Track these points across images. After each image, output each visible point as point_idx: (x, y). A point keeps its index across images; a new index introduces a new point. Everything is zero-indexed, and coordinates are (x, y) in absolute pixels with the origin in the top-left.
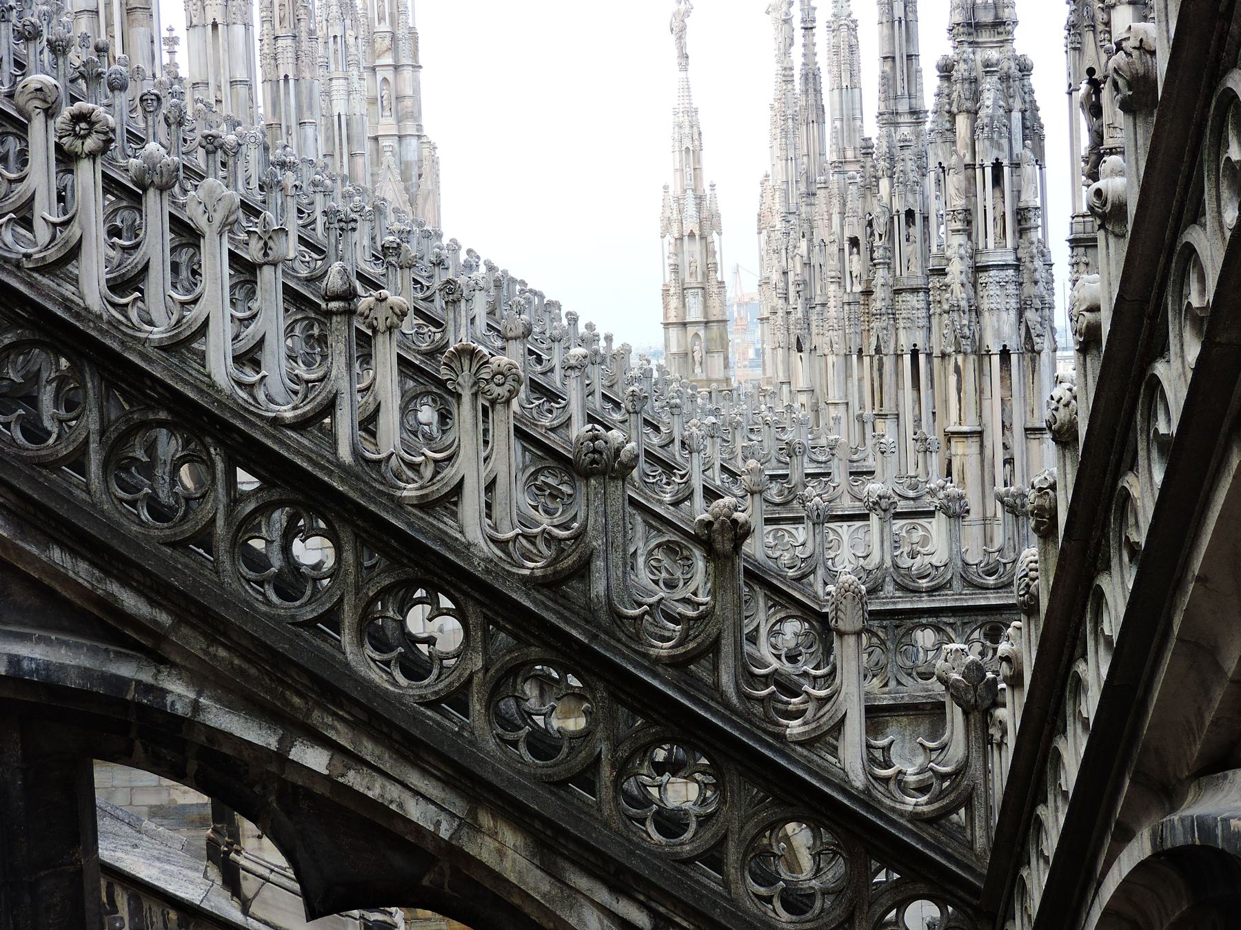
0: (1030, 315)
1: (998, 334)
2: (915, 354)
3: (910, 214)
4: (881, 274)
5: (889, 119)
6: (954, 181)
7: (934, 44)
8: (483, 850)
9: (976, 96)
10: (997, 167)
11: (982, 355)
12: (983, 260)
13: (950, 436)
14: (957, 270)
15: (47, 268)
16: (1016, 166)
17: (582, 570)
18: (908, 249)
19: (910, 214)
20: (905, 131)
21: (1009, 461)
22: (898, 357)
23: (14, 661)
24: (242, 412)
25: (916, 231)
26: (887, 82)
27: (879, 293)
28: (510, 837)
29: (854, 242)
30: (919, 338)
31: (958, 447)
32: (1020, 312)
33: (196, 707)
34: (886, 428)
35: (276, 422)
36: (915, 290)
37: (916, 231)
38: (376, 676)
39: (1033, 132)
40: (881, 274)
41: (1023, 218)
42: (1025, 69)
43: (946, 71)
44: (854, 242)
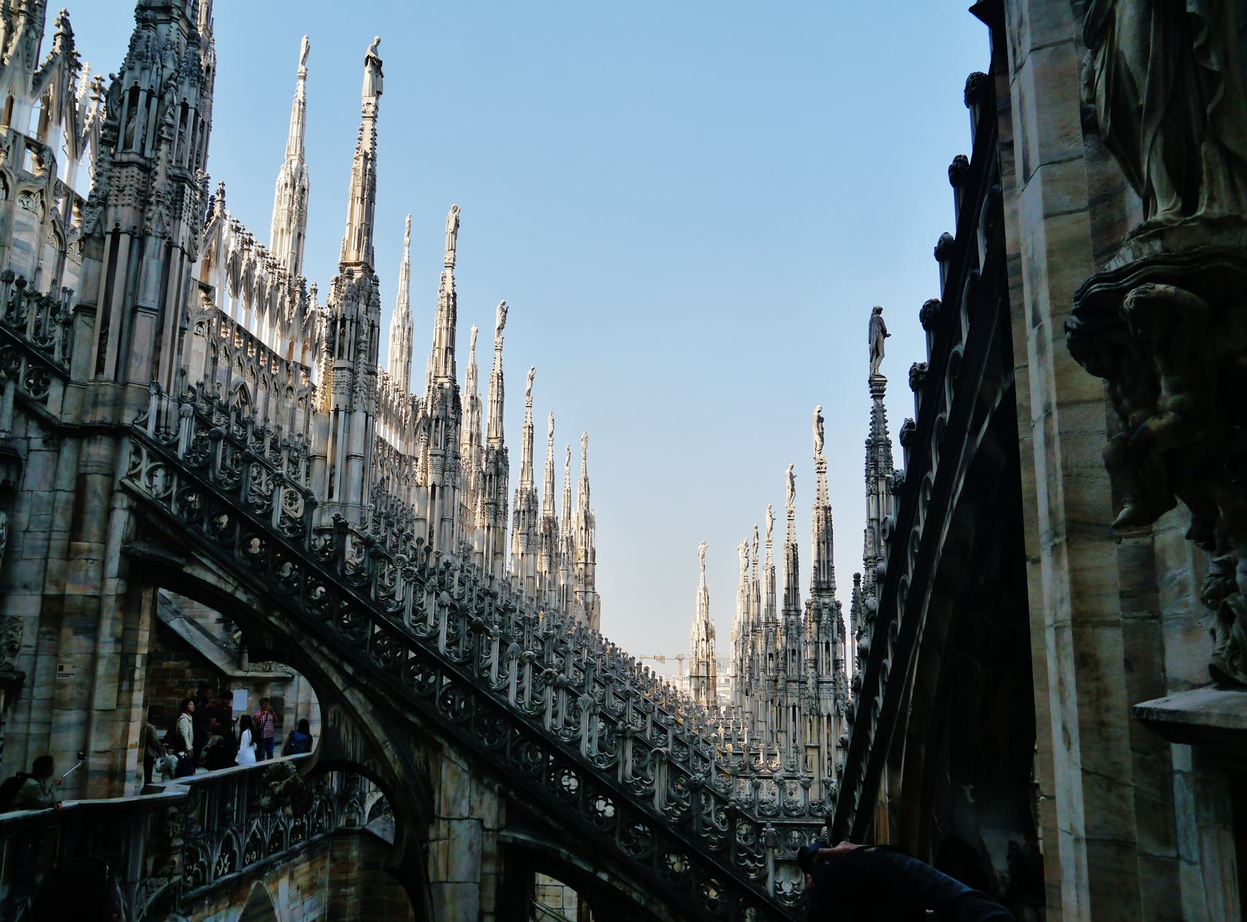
0: (839, 701)
1: (826, 708)
2: (794, 707)
3: (794, 651)
4: (782, 673)
5: (787, 612)
6: (810, 648)
7: (805, 594)
8: (655, 910)
9: (820, 616)
10: (827, 644)
11: (820, 716)
12: (821, 679)
13: (807, 747)
14: (811, 682)
15: (534, 717)
16: (835, 643)
17: (690, 821)
18: (792, 664)
19: (794, 651)
20: (793, 617)
21: (830, 759)
22: (787, 708)
23: (515, 839)
24: (589, 765)
25: (796, 658)
26: (787, 598)
27: (780, 681)
28: (663, 907)
29: (771, 655)
30: (796, 701)
31: (810, 752)
32: (835, 700)
33: (569, 857)
34: (782, 737)
35: (600, 769)
36: (794, 681)
37: (796, 658)
38: (625, 851)
39: (841, 630)
40: (782, 673)
41: (837, 664)
42: (839, 605)
43: (808, 605)
44: (771, 655)
